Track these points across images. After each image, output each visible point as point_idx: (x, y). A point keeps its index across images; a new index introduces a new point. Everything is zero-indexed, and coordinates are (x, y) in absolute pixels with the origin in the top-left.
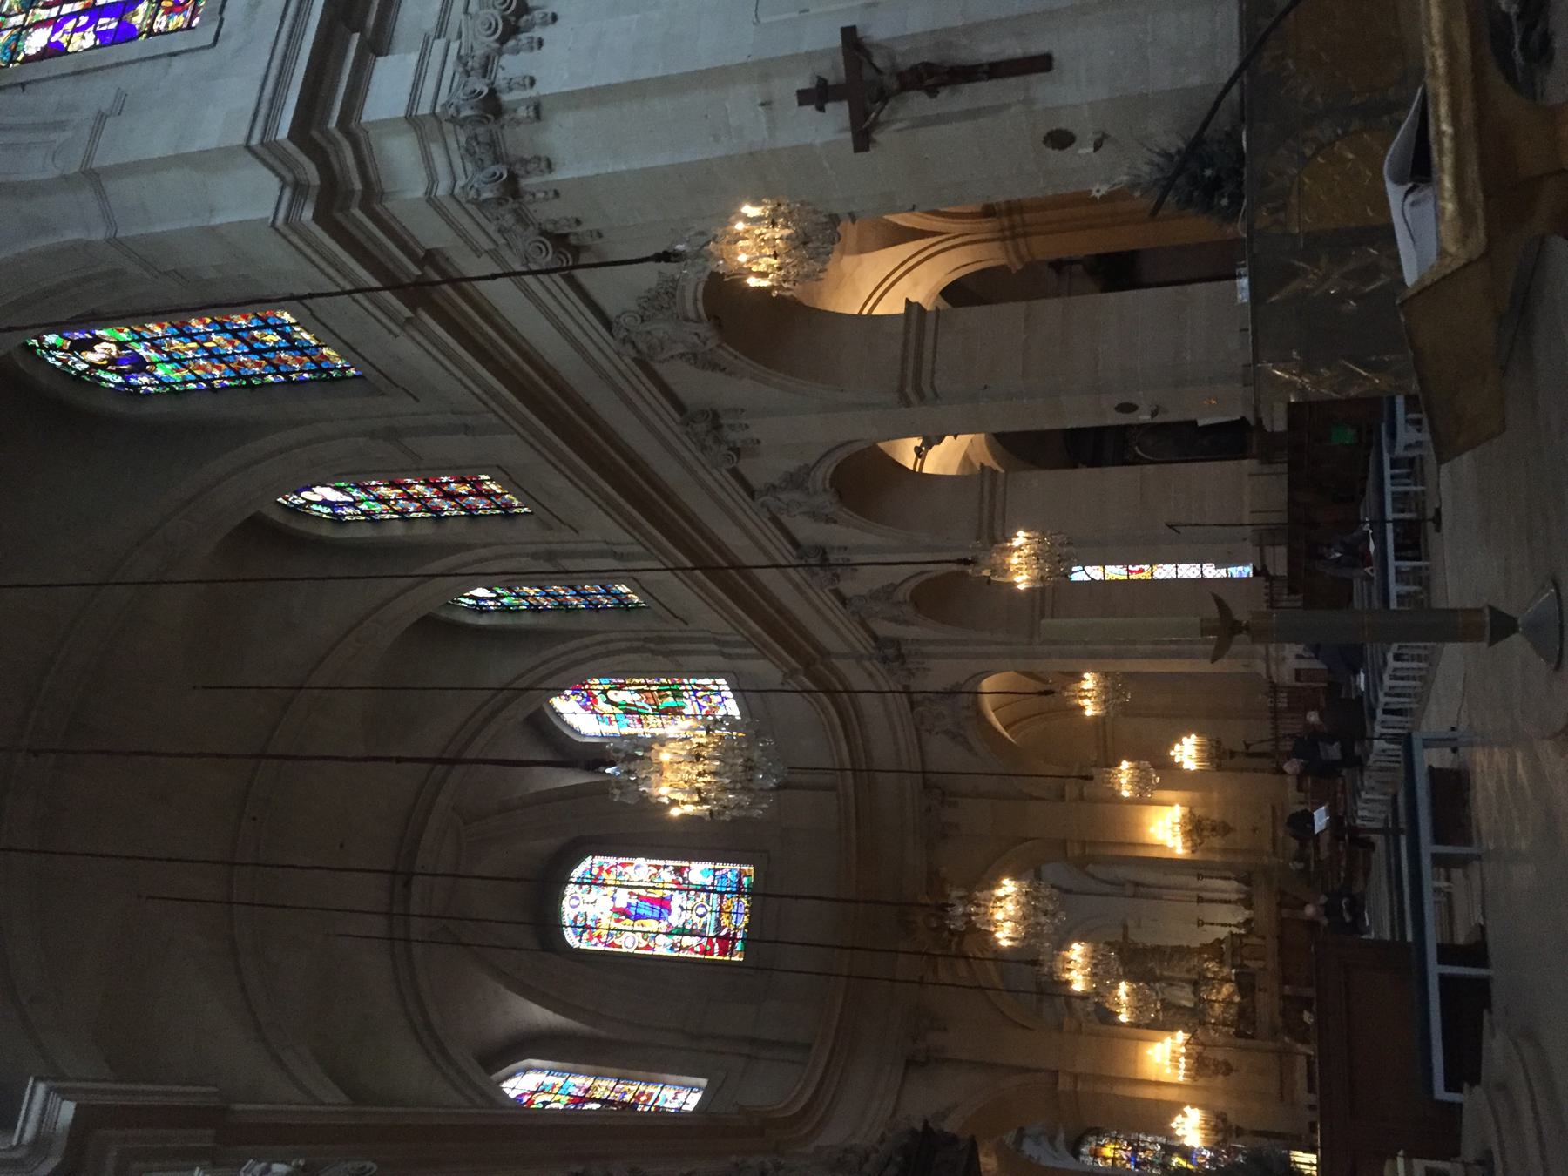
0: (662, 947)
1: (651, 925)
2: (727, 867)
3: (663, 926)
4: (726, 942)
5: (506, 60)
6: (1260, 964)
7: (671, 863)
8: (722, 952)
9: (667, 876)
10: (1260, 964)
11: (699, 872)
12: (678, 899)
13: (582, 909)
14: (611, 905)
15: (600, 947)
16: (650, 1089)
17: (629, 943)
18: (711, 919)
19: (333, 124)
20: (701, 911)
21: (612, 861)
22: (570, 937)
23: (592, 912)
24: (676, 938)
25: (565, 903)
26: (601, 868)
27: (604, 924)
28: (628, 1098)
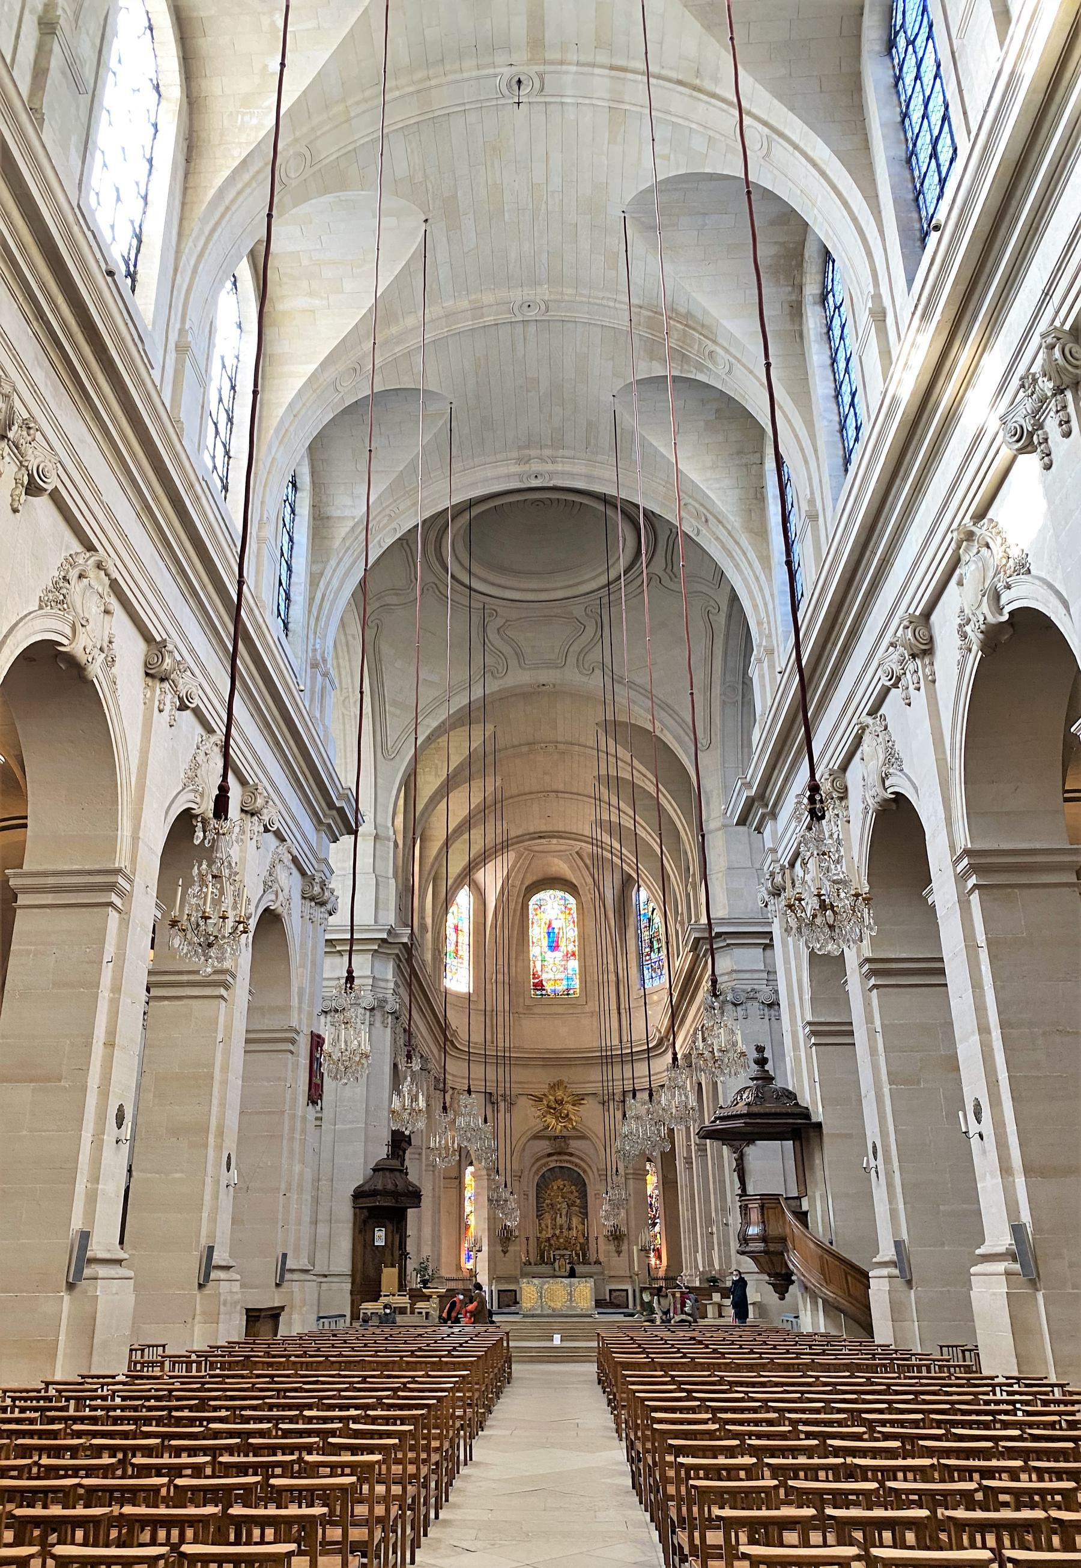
0: (534, 951)
1: (545, 943)
2: (578, 981)
3: (546, 949)
4: (539, 986)
5: (756, 1004)
6: (557, 1268)
7: (576, 949)
8: (535, 985)
9: (571, 948)
10: (557, 1268)
11: (574, 964)
12: (558, 955)
13: (550, 902)
14: (553, 918)
15: (531, 916)
16: (466, 962)
17: (537, 932)
18: (551, 976)
19: (728, 942)
20: (554, 969)
21: (575, 915)
22: (535, 899)
23: (548, 908)
24: (540, 958)
25: (552, 891)
26: (570, 909)
27: (543, 916)
28: (460, 953)
